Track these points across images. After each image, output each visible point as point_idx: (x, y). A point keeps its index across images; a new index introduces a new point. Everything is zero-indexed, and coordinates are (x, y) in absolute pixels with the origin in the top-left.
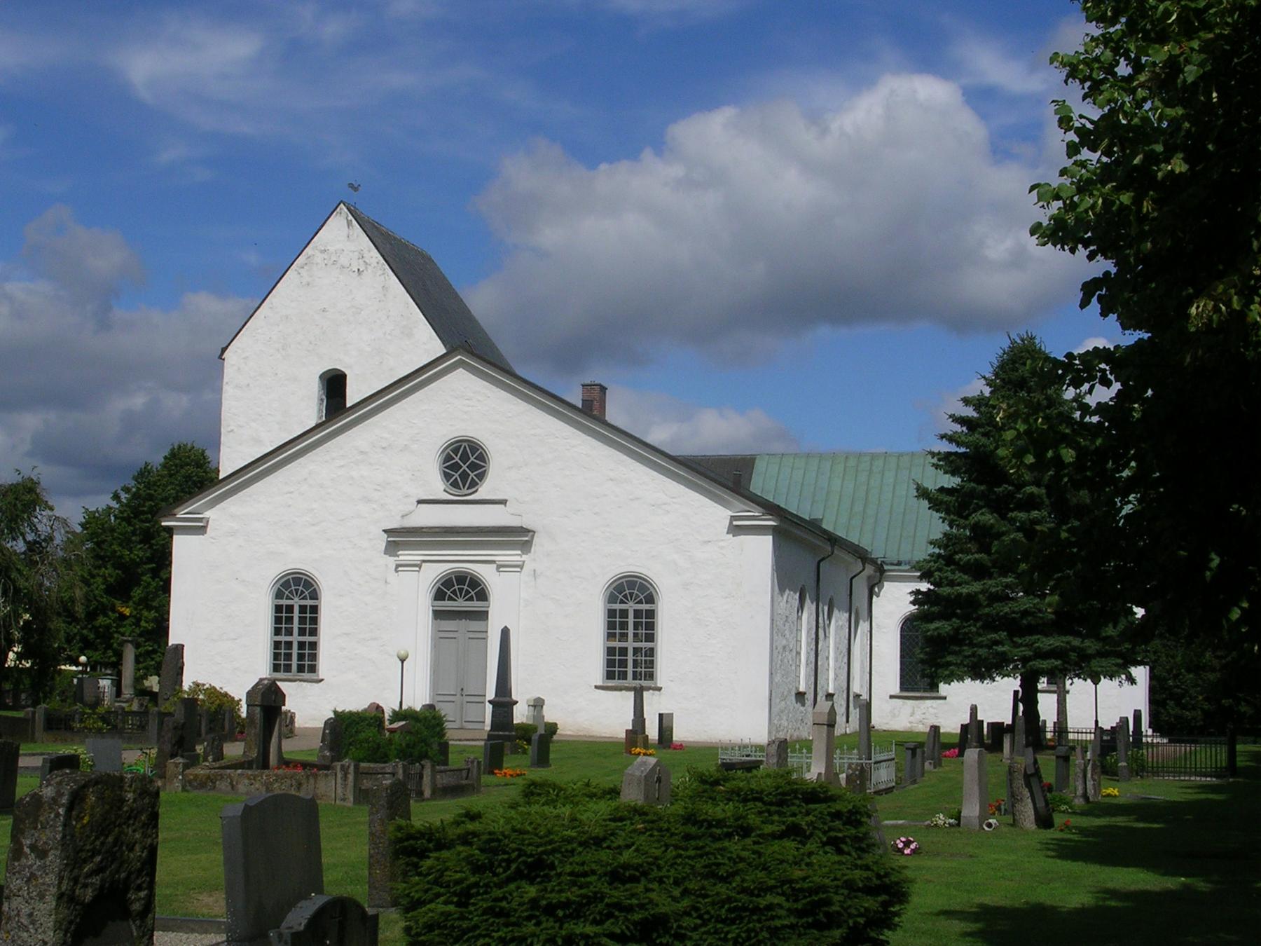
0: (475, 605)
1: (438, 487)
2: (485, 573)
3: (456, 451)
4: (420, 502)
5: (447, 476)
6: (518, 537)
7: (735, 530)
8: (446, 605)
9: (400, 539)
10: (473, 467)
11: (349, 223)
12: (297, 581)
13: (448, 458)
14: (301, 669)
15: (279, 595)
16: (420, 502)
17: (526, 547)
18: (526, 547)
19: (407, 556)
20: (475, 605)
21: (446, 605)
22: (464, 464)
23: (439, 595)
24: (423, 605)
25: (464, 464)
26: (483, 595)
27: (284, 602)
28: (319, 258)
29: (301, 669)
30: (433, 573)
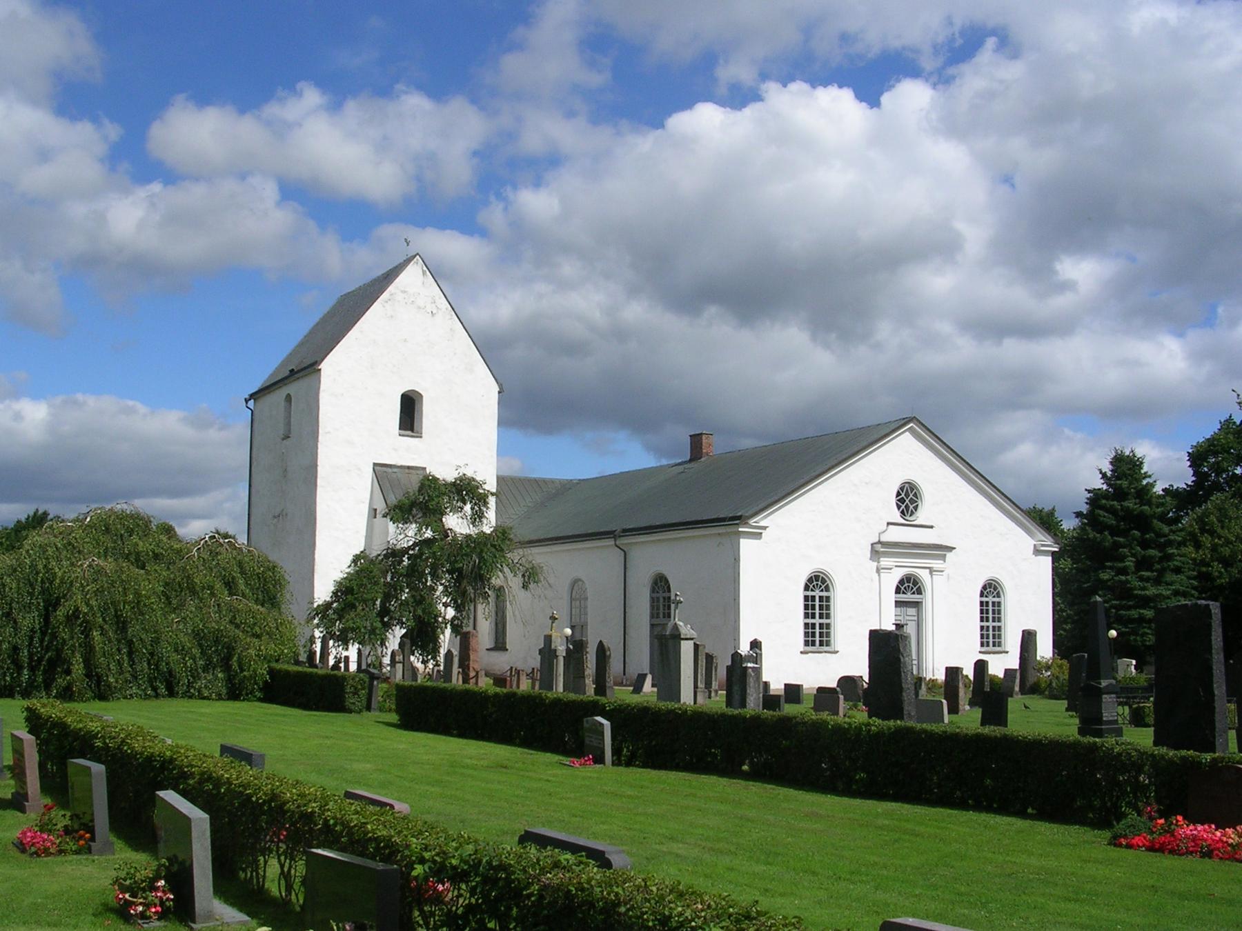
0: (916, 598)
1: (896, 516)
2: (924, 575)
3: (902, 489)
4: (889, 524)
5: (899, 507)
6: (941, 550)
7: (1037, 552)
8: (902, 597)
9: (880, 550)
10: (912, 501)
11: (424, 273)
12: (817, 577)
13: (898, 494)
14: (821, 644)
15: (807, 588)
16: (889, 524)
17: (943, 558)
18: (943, 558)
19: (885, 562)
20: (916, 598)
21: (902, 597)
22: (908, 498)
23: (898, 591)
24: (890, 597)
25: (908, 498)
26: (919, 592)
27: (810, 593)
28: (400, 297)
29: (821, 644)
30: (898, 574)
